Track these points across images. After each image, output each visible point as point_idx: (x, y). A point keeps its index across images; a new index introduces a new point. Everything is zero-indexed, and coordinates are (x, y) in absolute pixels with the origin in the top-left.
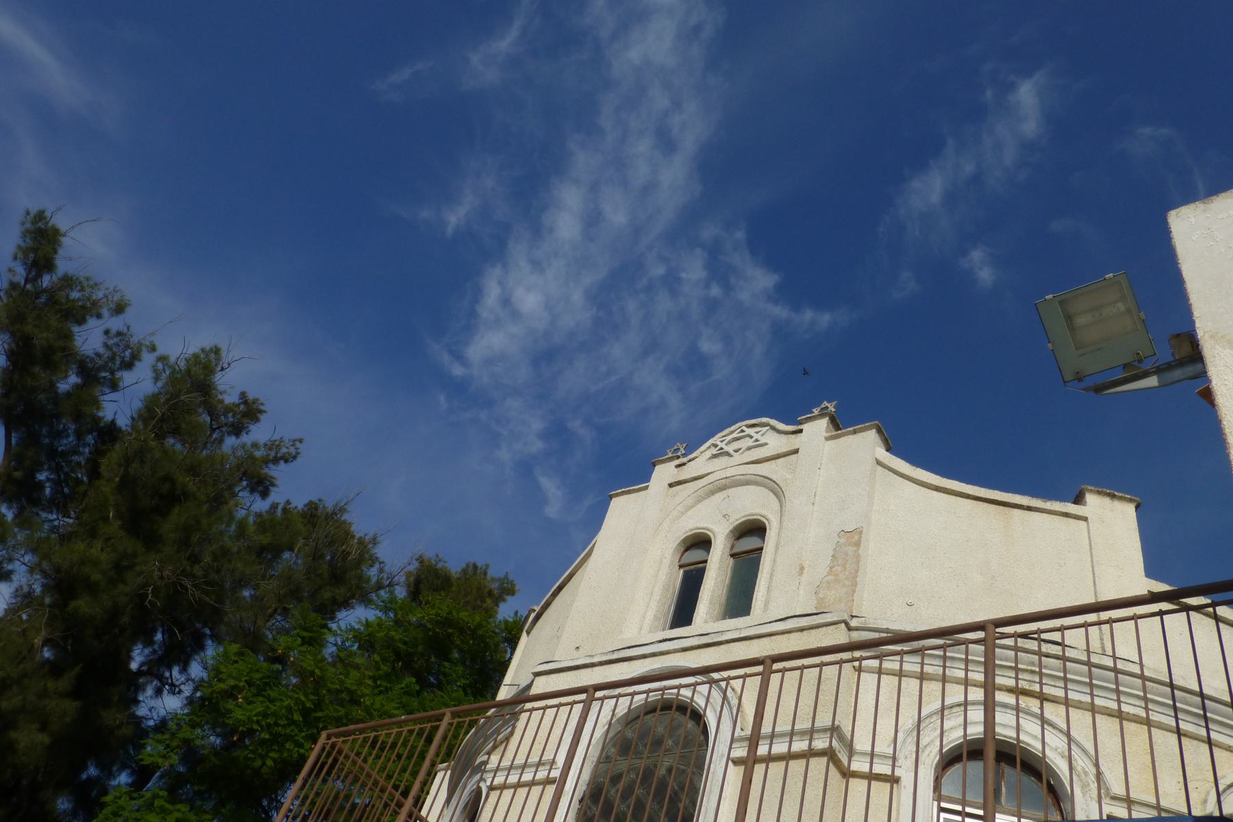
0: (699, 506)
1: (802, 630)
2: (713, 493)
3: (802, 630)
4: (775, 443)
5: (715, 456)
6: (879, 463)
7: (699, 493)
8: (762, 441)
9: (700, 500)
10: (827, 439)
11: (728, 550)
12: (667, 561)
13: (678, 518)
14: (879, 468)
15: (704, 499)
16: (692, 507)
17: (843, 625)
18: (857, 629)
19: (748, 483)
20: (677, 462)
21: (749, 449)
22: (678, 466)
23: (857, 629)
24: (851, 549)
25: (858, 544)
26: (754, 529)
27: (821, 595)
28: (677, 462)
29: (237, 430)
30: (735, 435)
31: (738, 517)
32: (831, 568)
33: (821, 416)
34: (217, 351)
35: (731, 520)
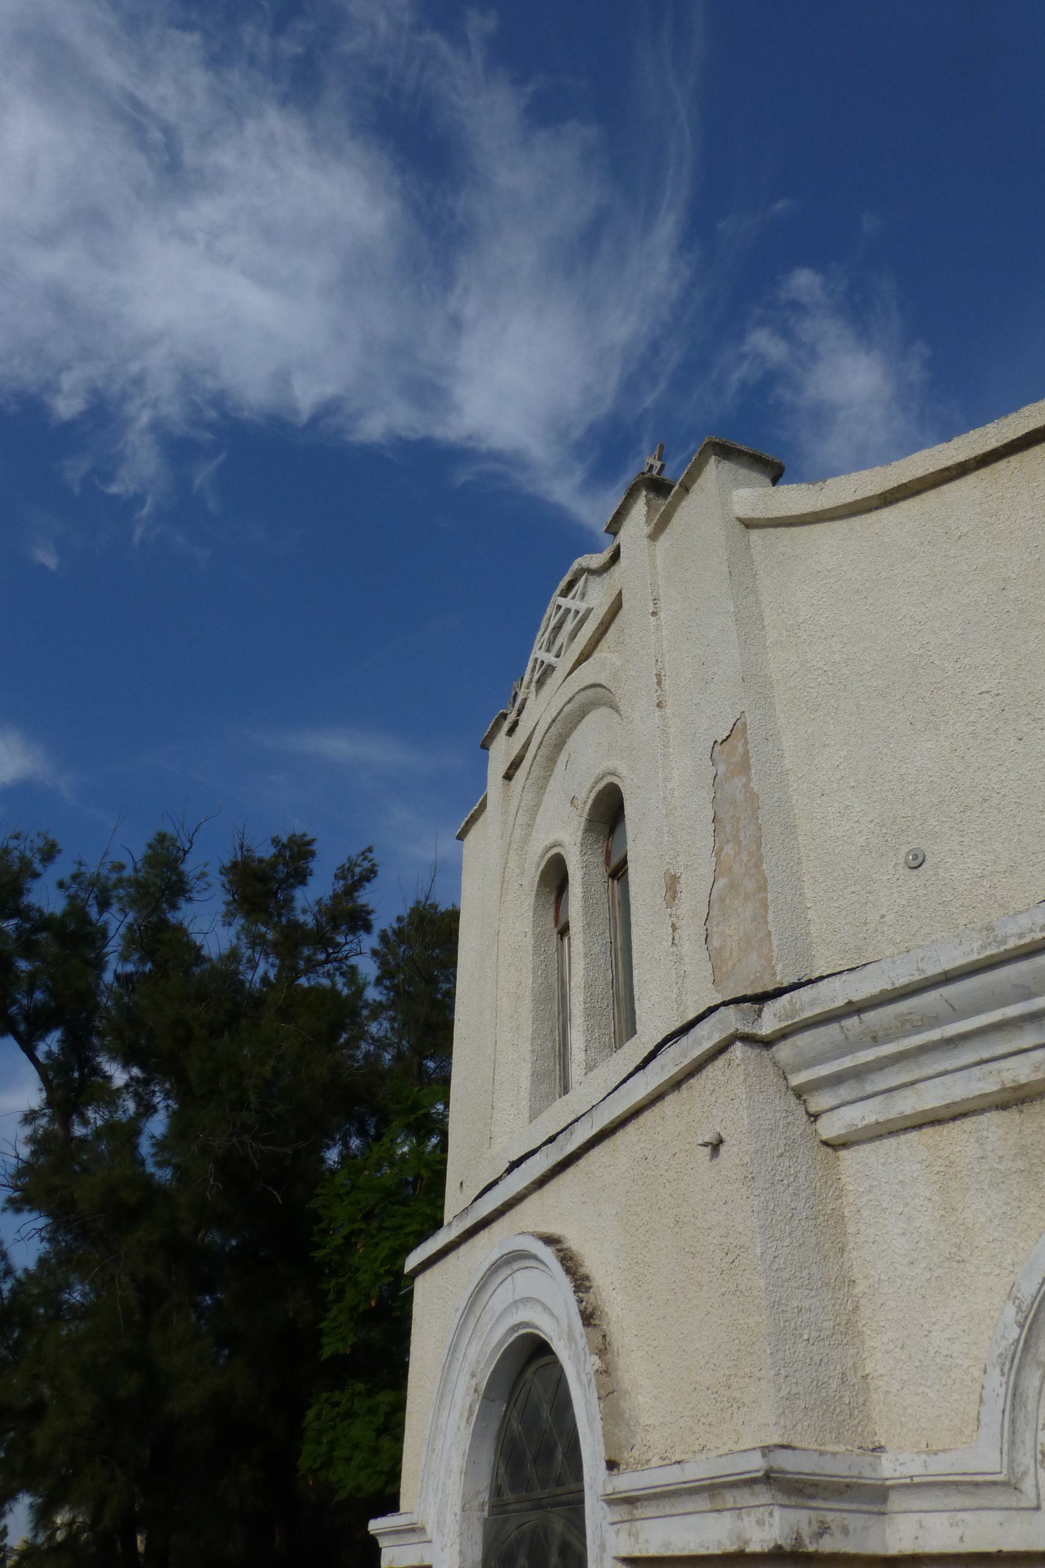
0: (545, 798)
1: (676, 1084)
2: (552, 760)
3: (676, 1084)
4: (595, 597)
5: (541, 683)
6: (749, 524)
7: (533, 775)
8: (583, 607)
9: (542, 787)
10: (654, 537)
11: (601, 872)
12: (529, 941)
13: (526, 839)
14: (755, 535)
15: (547, 778)
16: (538, 805)
17: (738, 1047)
18: (783, 1035)
19: (583, 712)
20: (506, 726)
21: (573, 636)
22: (511, 731)
23: (783, 1035)
24: (739, 781)
25: (745, 767)
26: (608, 812)
27: (716, 942)
28: (506, 726)
29: (301, 877)
30: (553, 623)
31: (586, 795)
32: (718, 855)
33: (631, 495)
34: (162, 838)
35: (579, 803)
